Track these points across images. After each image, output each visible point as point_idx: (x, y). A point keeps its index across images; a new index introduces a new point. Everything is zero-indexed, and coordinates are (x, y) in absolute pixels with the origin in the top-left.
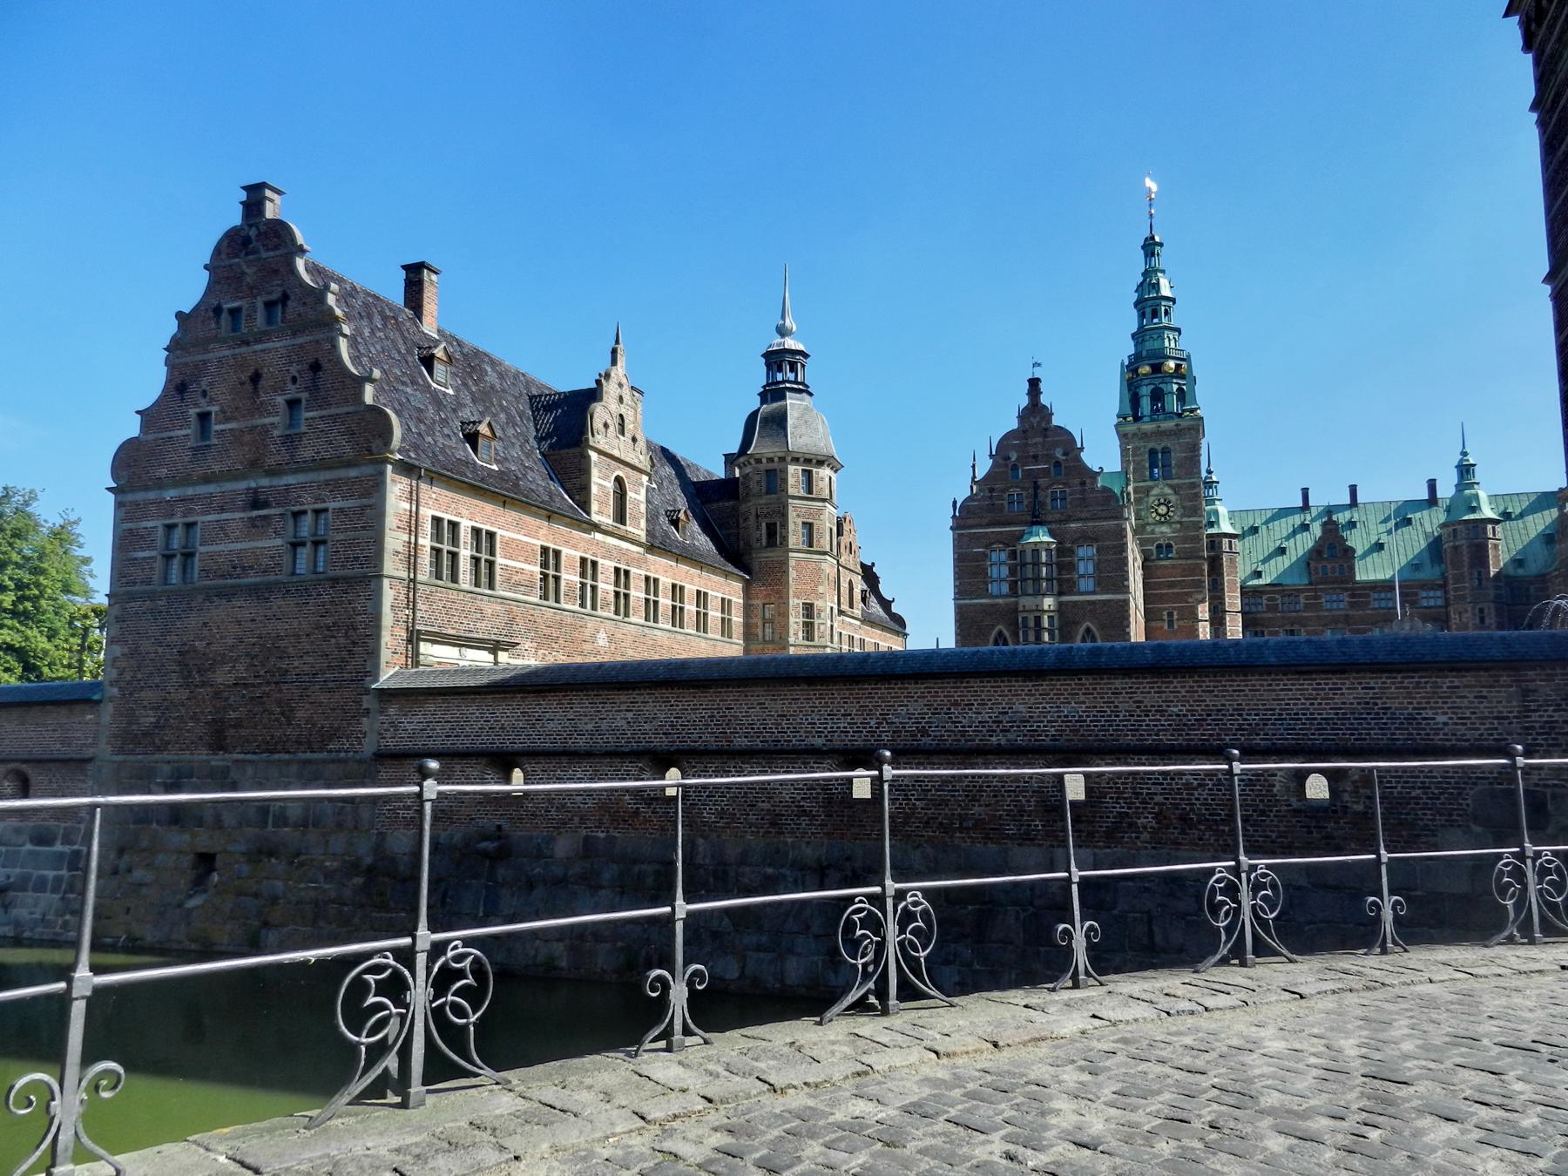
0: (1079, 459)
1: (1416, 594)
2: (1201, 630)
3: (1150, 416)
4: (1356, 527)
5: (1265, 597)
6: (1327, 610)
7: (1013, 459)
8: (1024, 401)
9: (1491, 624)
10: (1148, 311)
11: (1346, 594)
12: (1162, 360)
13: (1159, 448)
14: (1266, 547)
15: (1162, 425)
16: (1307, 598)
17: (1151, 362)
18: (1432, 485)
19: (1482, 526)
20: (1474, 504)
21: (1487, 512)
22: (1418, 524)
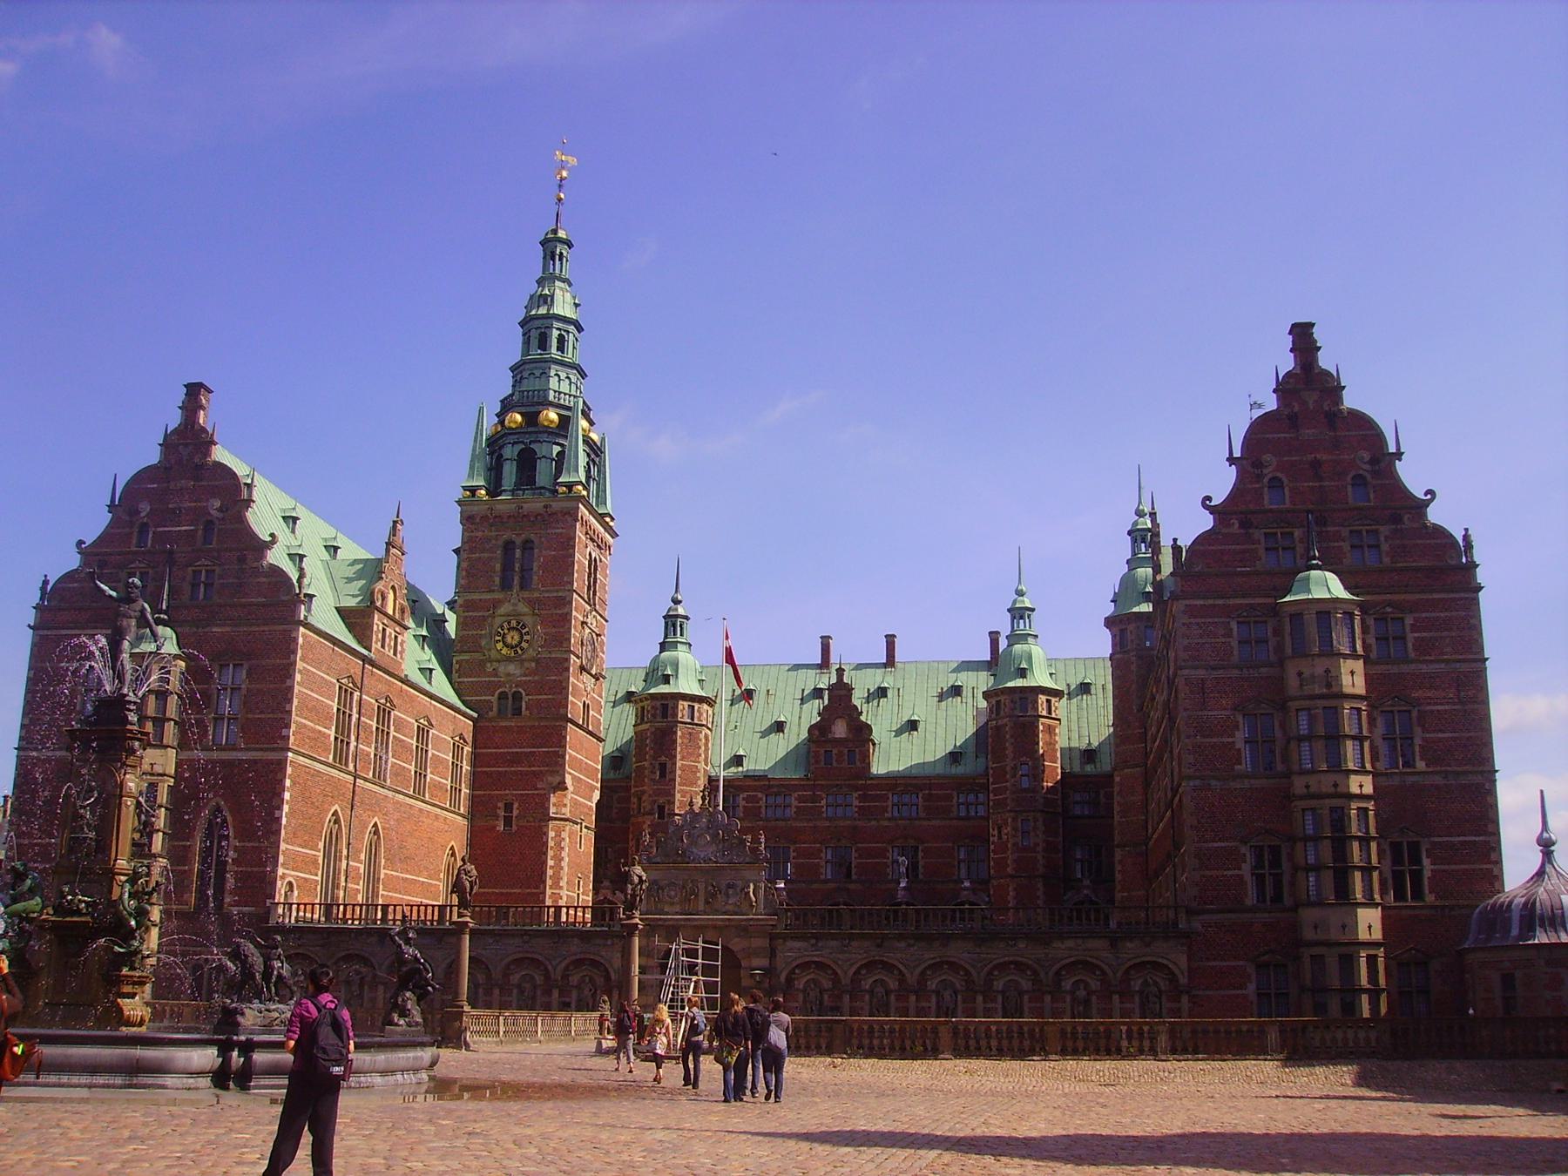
0: (242, 520)
2: (552, 834)
3: (513, 491)
6: (827, 819)
7: (143, 514)
8: (175, 419)
9: (1037, 845)
10: (534, 334)
11: (855, 795)
12: (541, 407)
13: (518, 541)
14: (759, 719)
15: (525, 506)
16: (799, 799)
17: (524, 410)
18: (994, 637)
20: (1024, 665)
21: (1040, 677)
22: (970, 695)
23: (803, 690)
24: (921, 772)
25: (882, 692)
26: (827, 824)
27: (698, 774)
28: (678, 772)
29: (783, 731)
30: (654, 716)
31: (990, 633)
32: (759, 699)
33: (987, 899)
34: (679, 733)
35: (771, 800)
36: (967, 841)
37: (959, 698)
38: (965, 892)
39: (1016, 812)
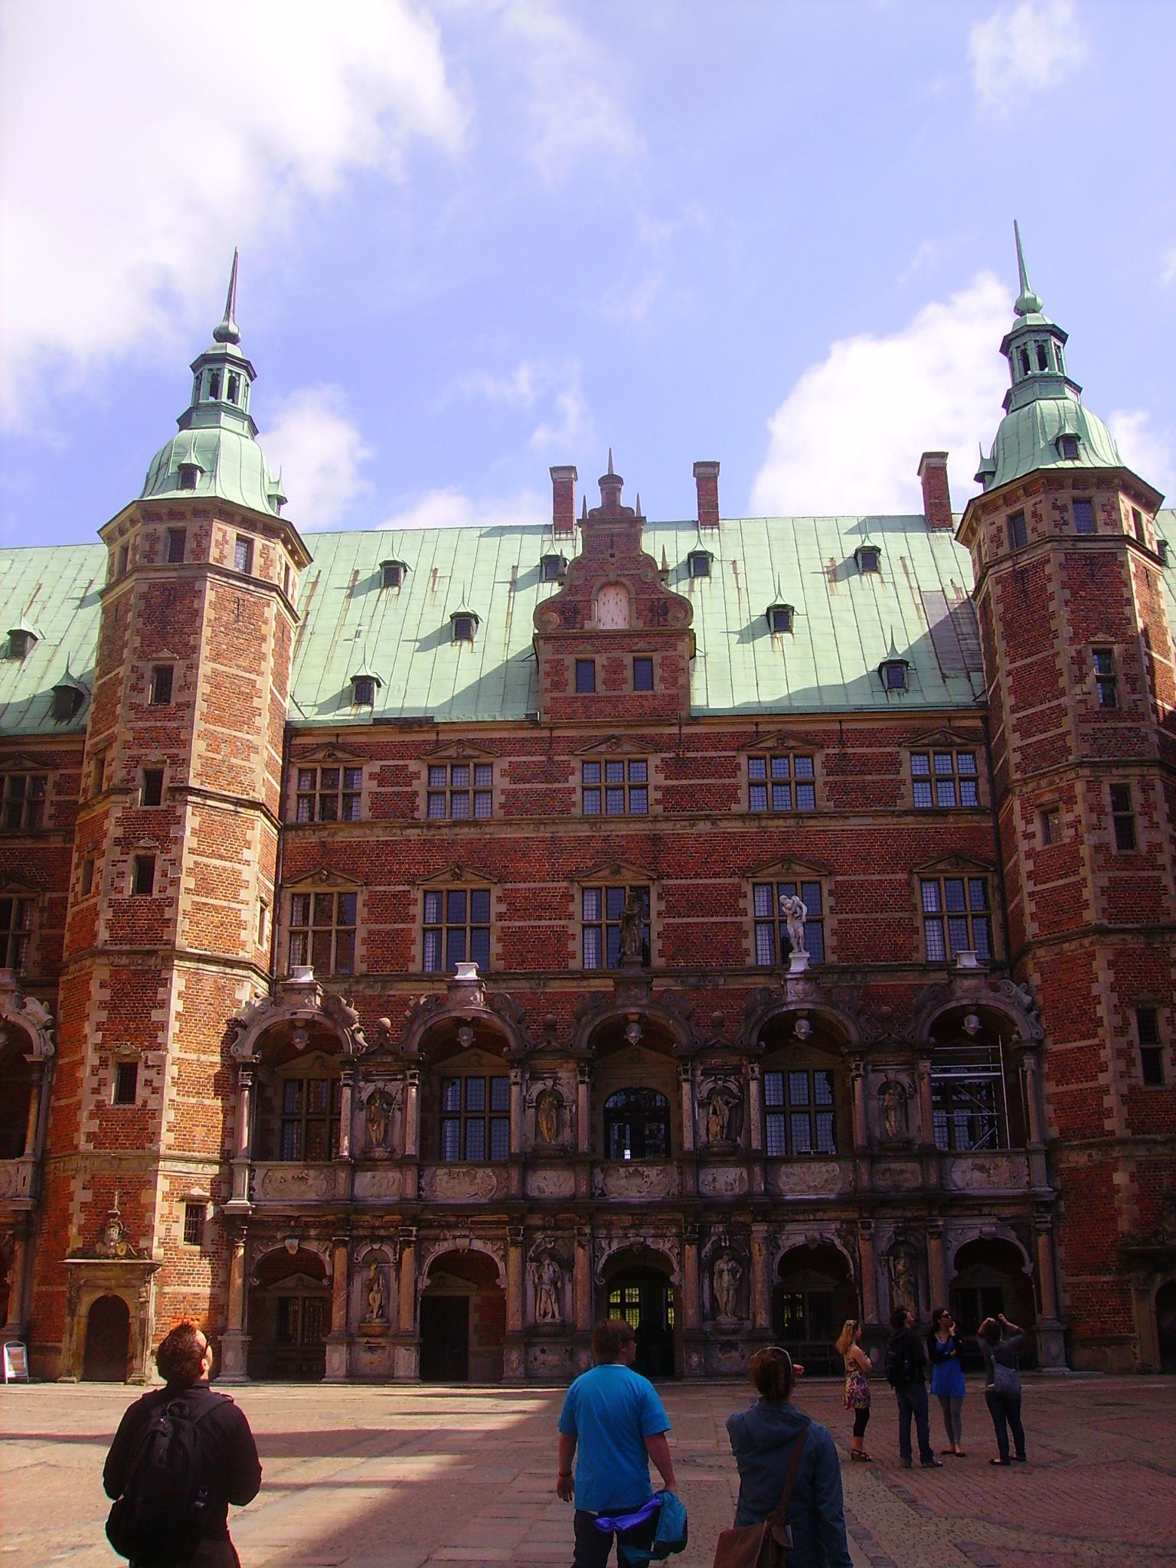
1: (894, 763)
4: (706, 573)
5: (375, 766)
6: (585, 819)
11: (654, 760)
14: (412, 620)
16: (516, 774)
19: (1099, 497)
20: (1069, 430)
22: (898, 568)
23: (515, 568)
24: (813, 704)
25: (699, 563)
26: (585, 831)
27: (256, 702)
28: (203, 688)
29: (470, 639)
30: (149, 556)
31: (926, 456)
32: (414, 583)
33: (1027, 999)
34: (210, 596)
35: (441, 781)
36: (940, 866)
37: (875, 576)
38: (968, 983)
39: (1093, 765)
